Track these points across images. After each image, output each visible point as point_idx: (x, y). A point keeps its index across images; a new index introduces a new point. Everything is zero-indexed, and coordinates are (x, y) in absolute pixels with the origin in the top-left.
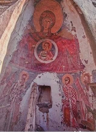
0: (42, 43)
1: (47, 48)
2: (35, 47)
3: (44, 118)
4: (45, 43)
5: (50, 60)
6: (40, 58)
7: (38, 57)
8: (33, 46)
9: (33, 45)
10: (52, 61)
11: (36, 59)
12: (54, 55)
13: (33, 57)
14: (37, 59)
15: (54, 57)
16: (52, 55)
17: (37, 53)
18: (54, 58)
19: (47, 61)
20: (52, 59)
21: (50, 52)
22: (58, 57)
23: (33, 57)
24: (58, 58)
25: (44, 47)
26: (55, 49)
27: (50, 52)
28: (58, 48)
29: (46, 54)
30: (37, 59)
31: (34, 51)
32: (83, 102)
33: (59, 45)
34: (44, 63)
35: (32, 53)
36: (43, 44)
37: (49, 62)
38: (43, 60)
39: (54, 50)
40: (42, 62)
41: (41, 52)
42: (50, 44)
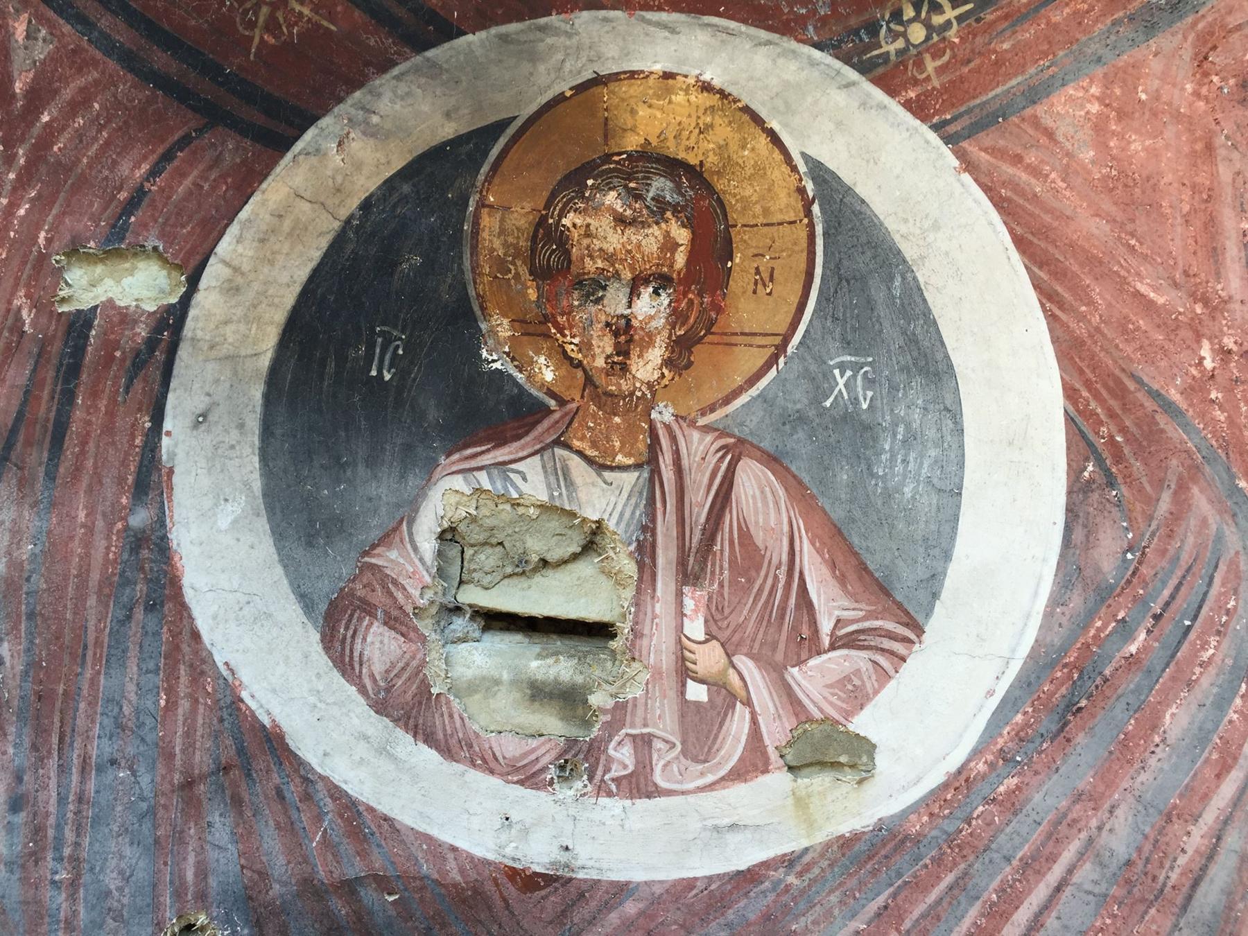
0: (439, 178)
1: (625, 335)
2: (171, 321)
3: (253, 696)
4: (574, 183)
5: (754, 763)
6: (413, 708)
7: (345, 661)
8: (89, 286)
9: (117, 245)
10: (851, 809)
11: (256, 754)
12: (895, 610)
13: (129, 683)
14: (273, 743)
15: (923, 665)
16: (831, 605)
17: (306, 511)
18: (932, 716)
19: (638, 785)
20: (830, 750)
21: (754, 485)
22: (1064, 695)
23: (129, 683)
24: (1087, 749)
25: (537, 328)
26: (929, 365)
27: (754, 485)
28: (1071, 351)
29: (593, 540)
30: (307, 744)
31: (150, 479)
32: (801, 522)
33: (1091, 227)
34: (537, 854)
35: (105, 549)
36: (500, 220)
37: (745, 855)
38: (530, 778)
39: (913, 407)
40: (470, 818)
41: (448, 494)
42: (759, 196)
